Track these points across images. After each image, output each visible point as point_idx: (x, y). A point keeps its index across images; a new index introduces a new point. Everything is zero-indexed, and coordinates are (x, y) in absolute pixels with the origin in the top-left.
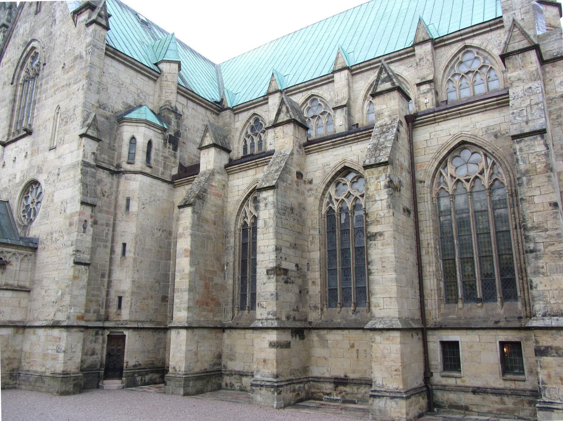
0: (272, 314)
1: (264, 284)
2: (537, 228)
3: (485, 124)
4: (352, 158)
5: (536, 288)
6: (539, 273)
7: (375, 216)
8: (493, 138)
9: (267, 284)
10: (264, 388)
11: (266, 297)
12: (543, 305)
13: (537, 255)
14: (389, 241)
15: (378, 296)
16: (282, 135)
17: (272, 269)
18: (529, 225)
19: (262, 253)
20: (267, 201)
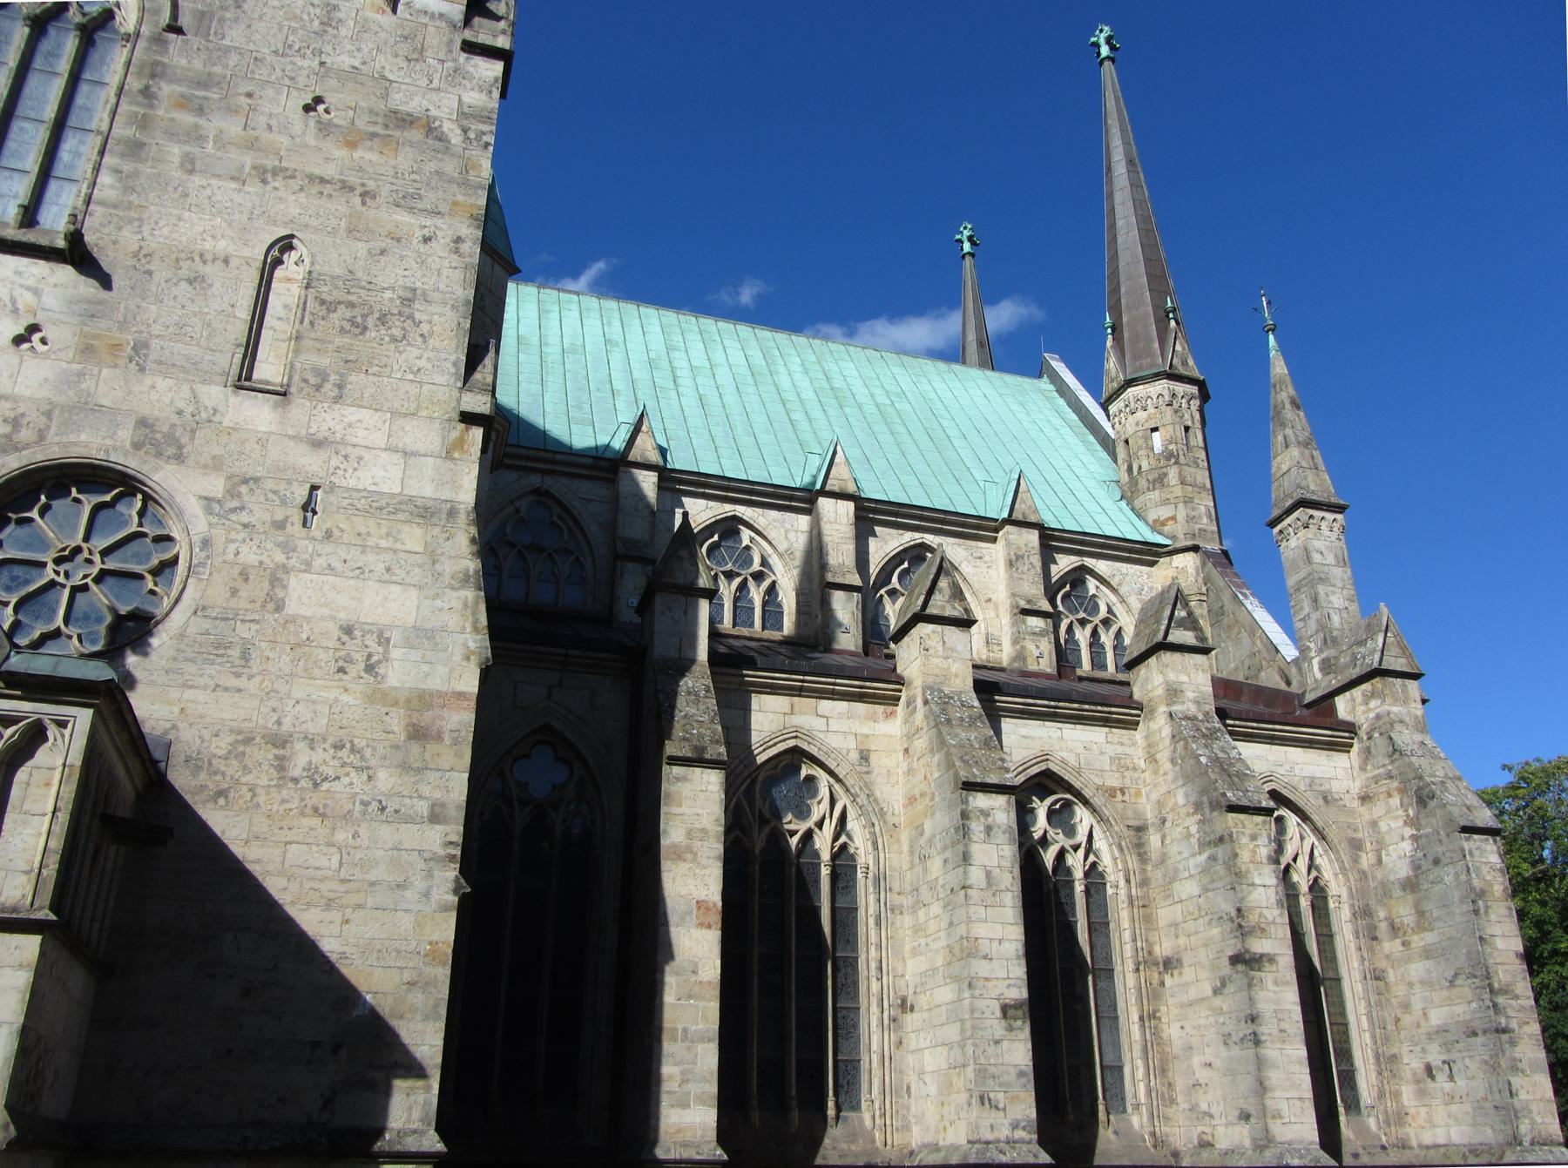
0: (1024, 1128)
1: (997, 1042)
2: (1506, 992)
3: (1309, 771)
4: (1065, 755)
5: (1517, 1095)
6: (1517, 1069)
7: (1257, 917)
8: (1321, 801)
9: (1005, 1044)
11: (1005, 1078)
12: (1529, 1126)
13: (1510, 1038)
14: (1288, 977)
15: (1277, 1094)
16: (940, 648)
17: (1017, 1005)
18: (1496, 985)
19: (985, 957)
20: (990, 820)
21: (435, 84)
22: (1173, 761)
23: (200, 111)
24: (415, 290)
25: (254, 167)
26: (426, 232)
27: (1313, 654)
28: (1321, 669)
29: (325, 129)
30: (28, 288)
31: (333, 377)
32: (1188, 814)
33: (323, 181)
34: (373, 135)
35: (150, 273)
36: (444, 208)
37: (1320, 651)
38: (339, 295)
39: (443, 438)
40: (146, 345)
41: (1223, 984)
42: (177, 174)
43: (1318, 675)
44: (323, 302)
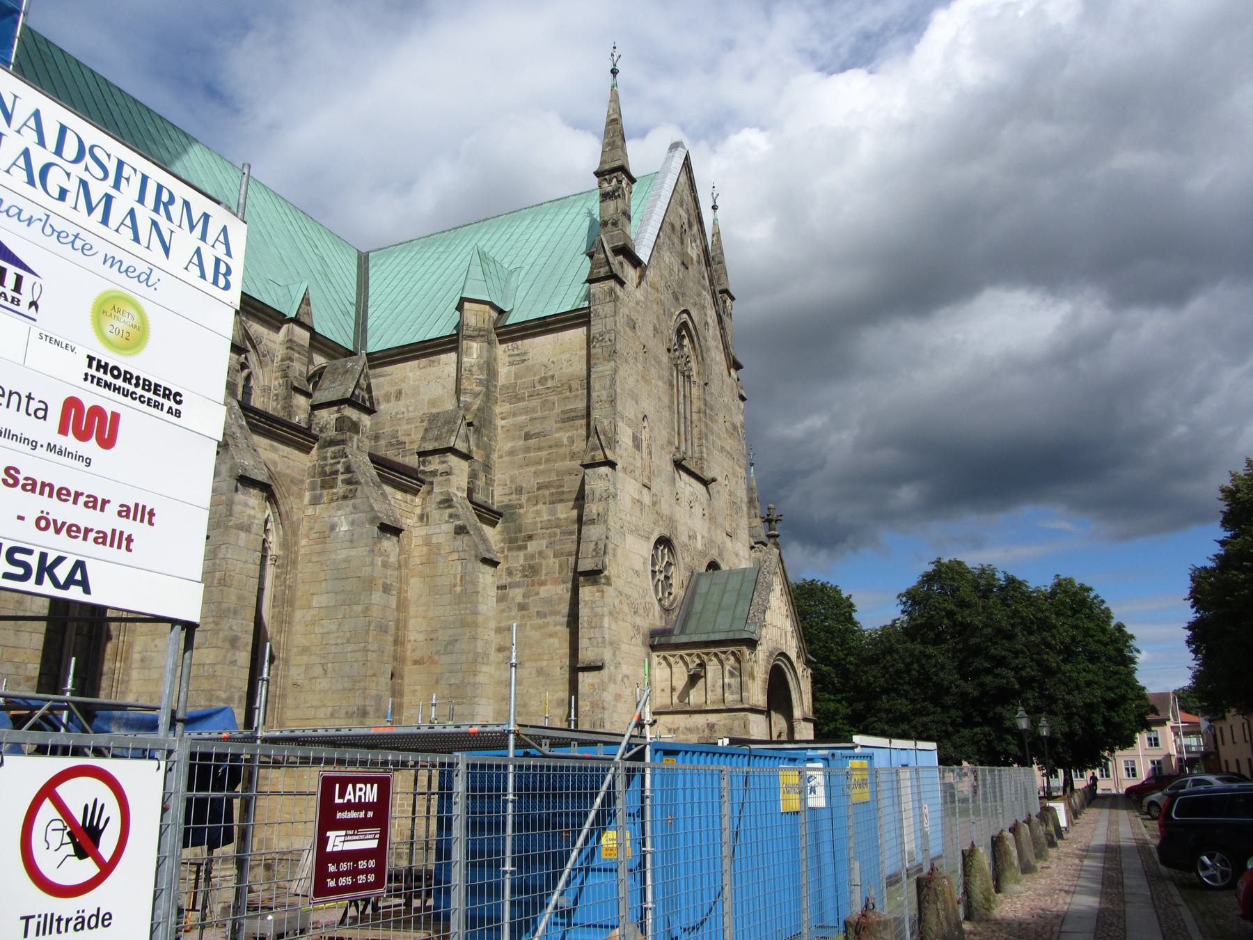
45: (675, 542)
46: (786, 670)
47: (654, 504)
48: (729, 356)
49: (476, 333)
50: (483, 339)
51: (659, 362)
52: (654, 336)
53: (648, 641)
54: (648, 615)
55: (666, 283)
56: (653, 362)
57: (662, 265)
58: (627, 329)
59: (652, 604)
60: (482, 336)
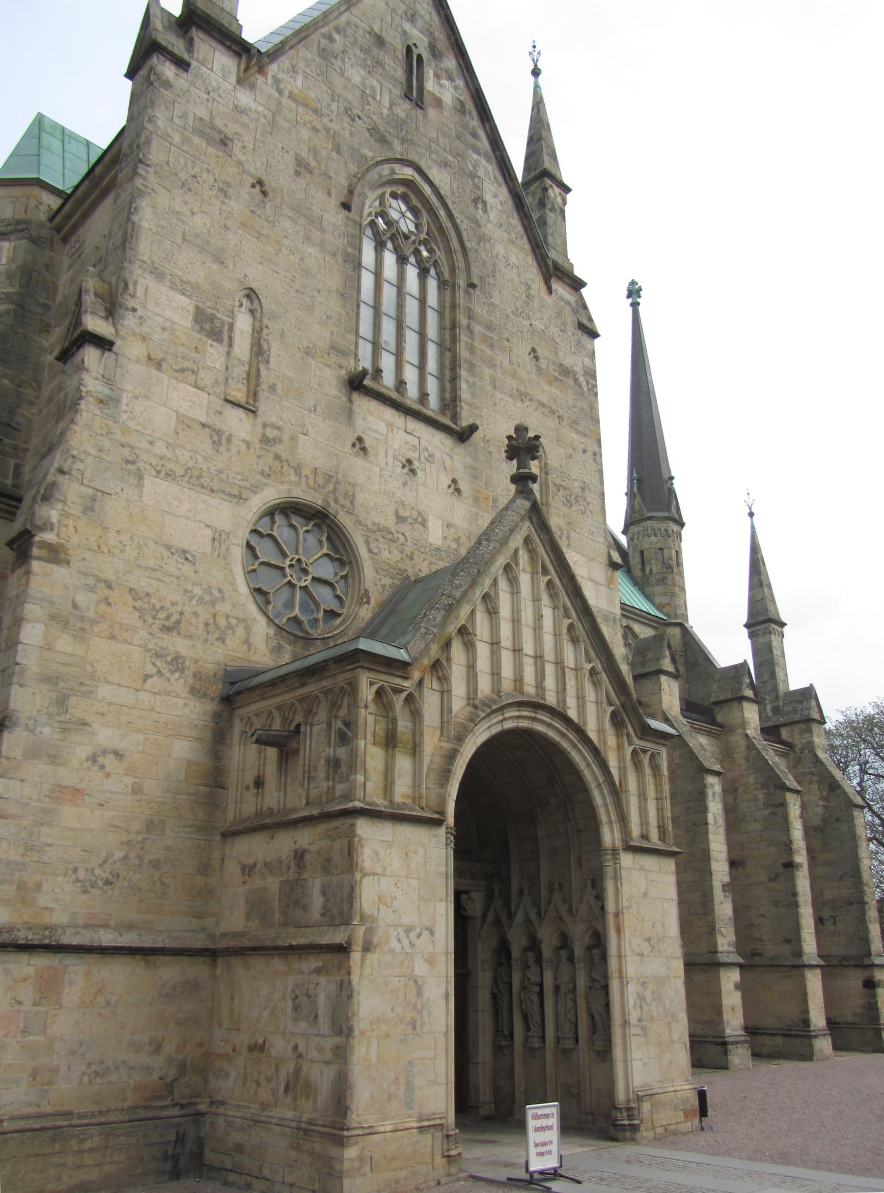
10: (739, 1046)
21: (573, 350)
22: (746, 760)
23: (491, 346)
24: (584, 482)
25: (518, 391)
26: (583, 446)
27: (767, 702)
28: (772, 711)
29: (539, 369)
30: (447, 454)
31: (565, 532)
32: (756, 789)
33: (544, 406)
34: (556, 379)
35: (490, 453)
36: (587, 432)
37: (772, 702)
38: (558, 481)
39: (606, 574)
40: (497, 501)
41: (777, 876)
42: (489, 388)
43: (770, 713)
44: (555, 485)
45: (345, 520)
46: (565, 744)
47: (266, 441)
48: (546, 265)
49: (10, 228)
50: (20, 235)
51: (315, 221)
52: (297, 174)
53: (217, 689)
54: (222, 640)
55: (347, 110)
56: (288, 212)
57: (338, 82)
58: (196, 140)
59: (244, 621)
60: (22, 230)
